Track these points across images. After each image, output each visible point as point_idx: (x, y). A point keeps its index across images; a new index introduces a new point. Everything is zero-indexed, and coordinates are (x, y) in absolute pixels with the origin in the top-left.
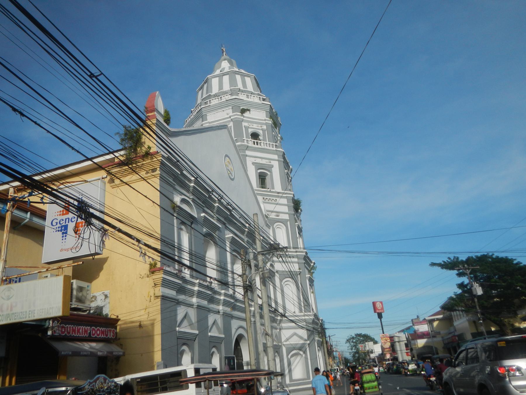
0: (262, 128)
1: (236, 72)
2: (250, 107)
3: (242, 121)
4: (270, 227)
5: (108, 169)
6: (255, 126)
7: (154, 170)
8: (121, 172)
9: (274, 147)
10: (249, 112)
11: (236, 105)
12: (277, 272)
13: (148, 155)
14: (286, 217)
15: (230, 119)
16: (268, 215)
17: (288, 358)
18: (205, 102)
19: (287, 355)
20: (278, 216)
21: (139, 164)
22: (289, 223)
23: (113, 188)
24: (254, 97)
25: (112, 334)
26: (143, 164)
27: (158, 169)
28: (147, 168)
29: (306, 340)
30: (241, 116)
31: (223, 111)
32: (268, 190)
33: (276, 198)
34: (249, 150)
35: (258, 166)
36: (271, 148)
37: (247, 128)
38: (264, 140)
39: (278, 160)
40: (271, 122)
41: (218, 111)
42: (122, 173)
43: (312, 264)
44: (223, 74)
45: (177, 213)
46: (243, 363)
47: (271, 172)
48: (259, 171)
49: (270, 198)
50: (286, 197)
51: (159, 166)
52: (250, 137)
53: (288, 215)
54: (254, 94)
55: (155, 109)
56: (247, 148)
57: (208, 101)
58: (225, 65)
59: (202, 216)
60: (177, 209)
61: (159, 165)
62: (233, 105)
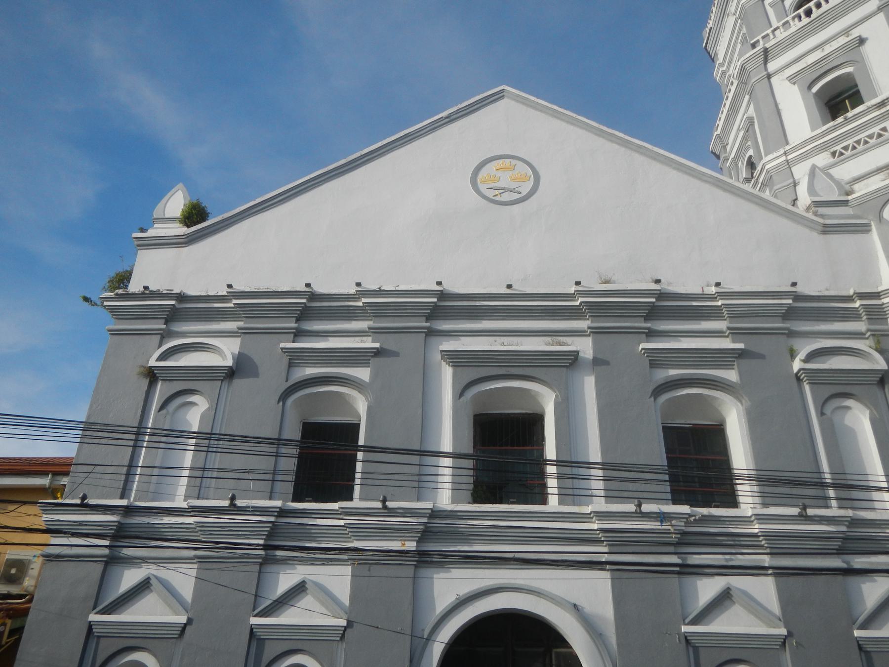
4: (868, 225)
45: (162, 380)
47: (860, 62)
48: (815, 89)
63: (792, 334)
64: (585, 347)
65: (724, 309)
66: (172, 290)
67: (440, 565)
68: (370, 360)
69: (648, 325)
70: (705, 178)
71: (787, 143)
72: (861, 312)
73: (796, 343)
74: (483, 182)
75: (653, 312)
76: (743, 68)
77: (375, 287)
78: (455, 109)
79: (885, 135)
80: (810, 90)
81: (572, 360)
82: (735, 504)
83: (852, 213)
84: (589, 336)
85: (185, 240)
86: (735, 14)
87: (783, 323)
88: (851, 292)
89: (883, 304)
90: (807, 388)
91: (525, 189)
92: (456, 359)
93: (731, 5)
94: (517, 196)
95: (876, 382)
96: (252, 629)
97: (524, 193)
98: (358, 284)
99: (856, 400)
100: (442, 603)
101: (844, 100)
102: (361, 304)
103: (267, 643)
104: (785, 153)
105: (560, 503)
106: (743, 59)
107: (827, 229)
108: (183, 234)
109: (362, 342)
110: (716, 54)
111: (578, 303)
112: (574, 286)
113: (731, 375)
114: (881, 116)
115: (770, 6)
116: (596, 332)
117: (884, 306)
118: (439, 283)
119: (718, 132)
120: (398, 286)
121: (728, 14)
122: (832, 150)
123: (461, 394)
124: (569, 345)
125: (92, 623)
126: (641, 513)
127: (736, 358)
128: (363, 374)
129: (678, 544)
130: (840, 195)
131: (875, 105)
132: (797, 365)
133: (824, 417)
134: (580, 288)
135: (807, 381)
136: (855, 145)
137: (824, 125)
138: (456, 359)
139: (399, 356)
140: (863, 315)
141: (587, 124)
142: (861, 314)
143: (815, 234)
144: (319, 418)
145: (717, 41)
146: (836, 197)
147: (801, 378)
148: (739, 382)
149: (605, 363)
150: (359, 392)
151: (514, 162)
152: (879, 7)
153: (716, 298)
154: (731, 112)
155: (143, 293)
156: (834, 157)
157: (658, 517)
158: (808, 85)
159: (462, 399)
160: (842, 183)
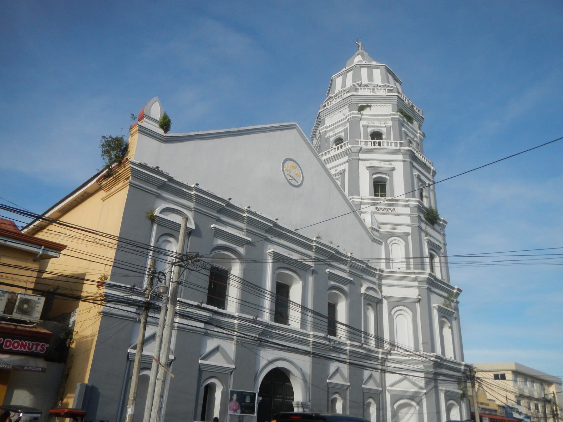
0: (386, 124)
1: (361, 66)
2: (371, 103)
3: (360, 121)
4: (382, 243)
5: (99, 182)
6: (377, 123)
7: (128, 178)
8: (108, 184)
9: (398, 145)
10: (369, 108)
12: (384, 297)
13: (121, 164)
14: (408, 230)
15: (346, 120)
16: (379, 228)
17: (394, 409)
18: (323, 105)
19: (393, 404)
20: (395, 229)
21: (117, 174)
22: (410, 238)
23: (103, 201)
24: (381, 91)
25: (39, 348)
26: (119, 174)
27: (131, 177)
28: (123, 177)
29: (421, 388)
30: (359, 114)
31: (340, 112)
32: (382, 198)
33: (394, 208)
34: (363, 153)
35: (373, 170)
37: (366, 127)
38: (389, 138)
39: (402, 161)
40: (398, 116)
41: (336, 112)
42: (109, 186)
43: (455, 291)
44: (347, 71)
45: (157, 224)
46: (293, 403)
47: (391, 176)
48: (375, 176)
49: (385, 207)
51: (131, 174)
52: (370, 137)
53: (410, 228)
54: (380, 87)
55: (144, 115)
56: (361, 150)
57: (326, 104)
58: (357, 59)
59: (211, 227)
60: (156, 219)
61: (130, 171)
64: (310, 263)
66: (169, 174)
67: (263, 346)
68: (245, 245)
70: (349, 204)
73: (362, 281)
77: (254, 211)
81: (306, 268)
85: (165, 139)
88: (378, 268)
89: (383, 275)
90: (362, 299)
92: (277, 257)
96: (199, 365)
97: (299, 184)
99: (371, 306)
100: (263, 363)
101: (378, 185)
103: (203, 373)
104: (361, 199)
105: (301, 328)
107: (374, 240)
108: (165, 136)
110: (324, 119)
116: (317, 260)
125: (129, 354)
128: (241, 250)
129: (330, 350)
132: (363, 290)
134: (317, 240)
138: (277, 257)
143: (370, 240)
146: (376, 228)
149: (317, 273)
151: (296, 165)
155: (154, 169)
160: (378, 222)
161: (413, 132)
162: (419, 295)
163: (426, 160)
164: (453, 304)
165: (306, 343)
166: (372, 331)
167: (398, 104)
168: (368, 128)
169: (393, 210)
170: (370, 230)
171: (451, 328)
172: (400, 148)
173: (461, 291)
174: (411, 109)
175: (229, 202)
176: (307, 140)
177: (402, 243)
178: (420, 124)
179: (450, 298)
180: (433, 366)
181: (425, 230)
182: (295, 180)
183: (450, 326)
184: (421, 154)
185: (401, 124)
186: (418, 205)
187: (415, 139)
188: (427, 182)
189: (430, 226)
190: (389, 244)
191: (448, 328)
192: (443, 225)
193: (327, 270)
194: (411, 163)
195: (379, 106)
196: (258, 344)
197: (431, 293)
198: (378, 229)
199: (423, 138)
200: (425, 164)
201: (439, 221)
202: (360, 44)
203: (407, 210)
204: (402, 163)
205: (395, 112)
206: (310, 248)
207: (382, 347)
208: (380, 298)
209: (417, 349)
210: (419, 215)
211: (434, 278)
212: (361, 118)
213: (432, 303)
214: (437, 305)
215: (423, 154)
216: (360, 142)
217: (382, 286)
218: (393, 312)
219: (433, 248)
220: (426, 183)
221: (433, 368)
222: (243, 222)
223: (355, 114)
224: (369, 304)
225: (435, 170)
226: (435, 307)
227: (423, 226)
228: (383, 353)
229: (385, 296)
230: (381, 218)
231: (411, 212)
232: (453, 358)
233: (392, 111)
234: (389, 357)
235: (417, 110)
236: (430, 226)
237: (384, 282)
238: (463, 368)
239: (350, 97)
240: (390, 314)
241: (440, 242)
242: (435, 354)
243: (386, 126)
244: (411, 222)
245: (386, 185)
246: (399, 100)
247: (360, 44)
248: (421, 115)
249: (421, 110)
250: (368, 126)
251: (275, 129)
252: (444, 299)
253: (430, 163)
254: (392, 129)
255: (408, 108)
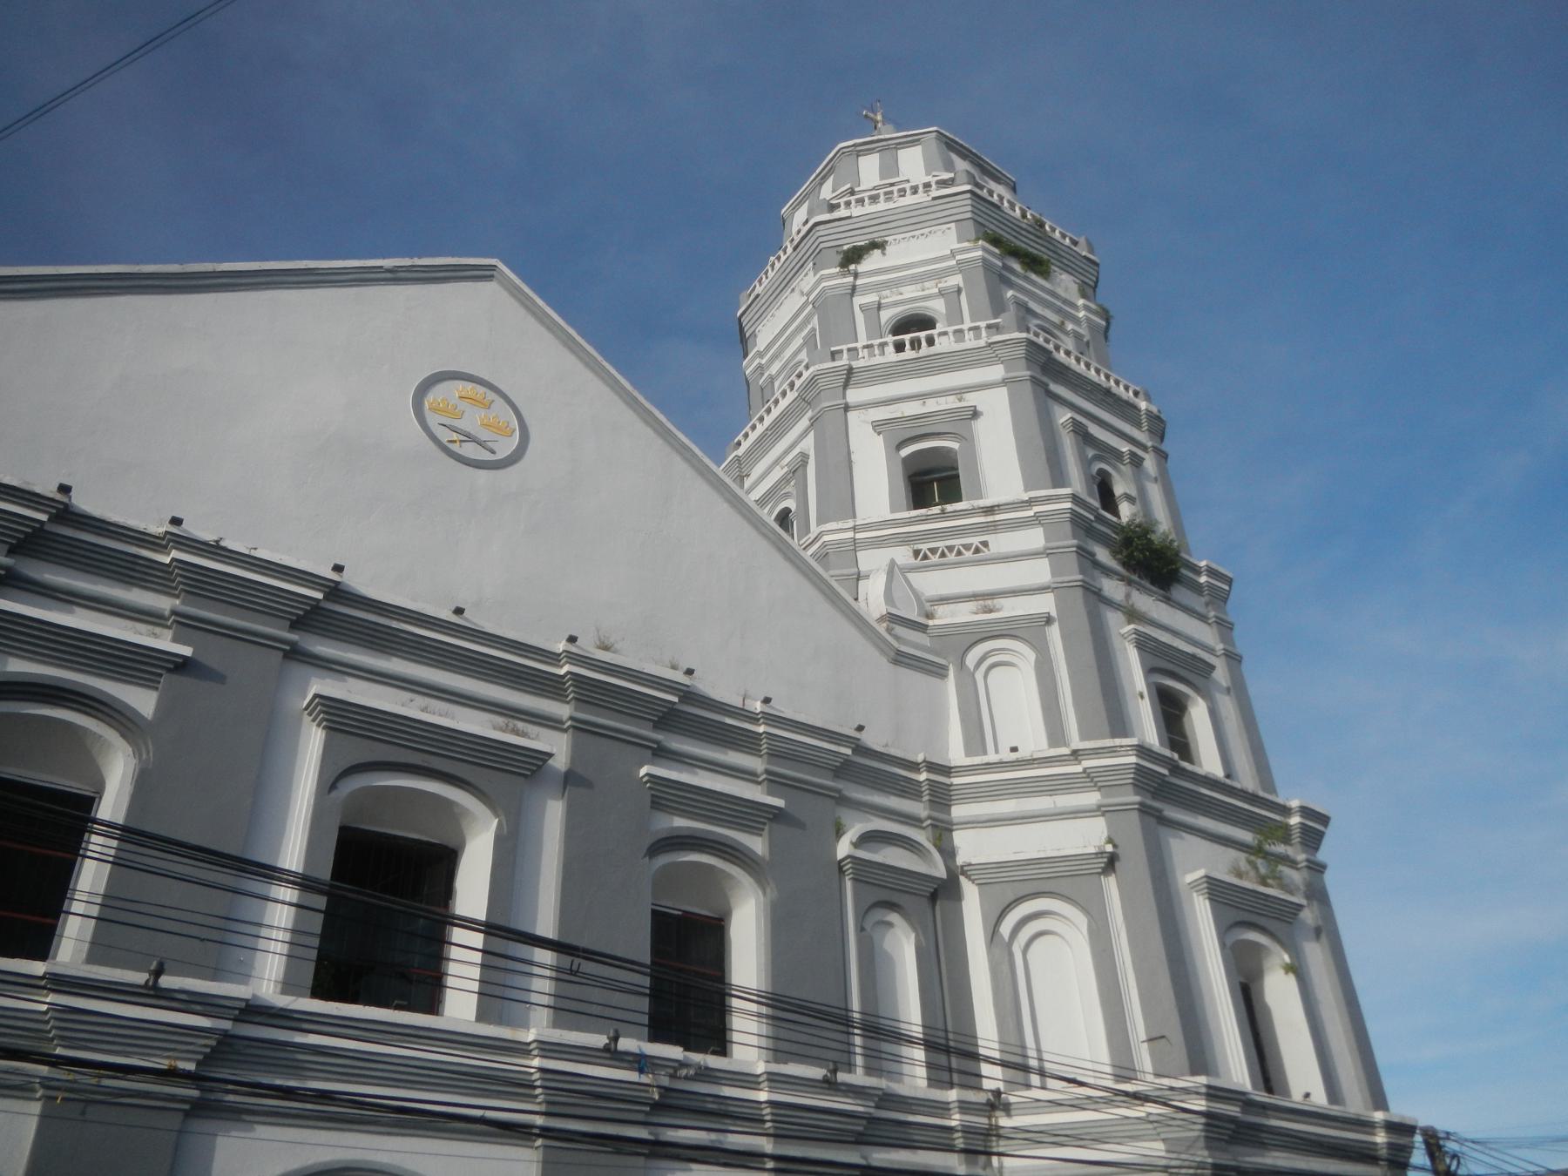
4: (945, 668)
6: (910, 292)
10: (880, 251)
11: (822, 246)
14: (1045, 604)
15: (811, 306)
16: (930, 616)
20: (991, 611)
22: (1054, 632)
30: (844, 276)
31: (793, 290)
32: (930, 513)
36: (970, 342)
40: (979, 253)
43: (1295, 820)
47: (967, 439)
49: (949, 543)
50: (1037, 520)
62: (812, 256)
63: (843, 800)
64: (558, 747)
65: (764, 741)
67: (237, 1115)
68: (161, 675)
69: (659, 736)
71: (854, 516)
72: (923, 789)
73: (846, 815)
74: (434, 410)
75: (668, 719)
76: (813, 380)
77: (209, 537)
78: (406, 262)
79: (984, 552)
80: (899, 451)
81: (532, 764)
82: (722, 1048)
83: (929, 645)
84: (565, 731)
86: (808, 295)
87: (833, 781)
88: (920, 758)
89: (951, 785)
90: (849, 885)
91: (505, 448)
92: (337, 716)
93: (802, 279)
94: (486, 456)
95: (928, 894)
97: (500, 456)
98: (176, 521)
99: (902, 915)
101: (931, 482)
102: (167, 560)
104: (854, 528)
105: (482, 1016)
106: (817, 367)
107: (901, 659)
109: (155, 635)
110: (754, 335)
111: (562, 672)
112: (564, 642)
113: (757, 844)
114: (986, 525)
115: (861, 309)
116: (580, 728)
117: (952, 788)
118: (338, 569)
119: (741, 451)
120: (255, 549)
121: (793, 290)
122: (916, 547)
123: (333, 787)
124: (533, 739)
126: (616, 1052)
127: (769, 819)
128: (142, 701)
129: (657, 1107)
130: (919, 615)
131: (983, 508)
132: (844, 848)
133: (863, 933)
134: (573, 649)
135: (851, 876)
136: (946, 551)
137: (909, 509)
138: (337, 716)
139: (223, 683)
140: (925, 793)
141: (617, 381)
142: (922, 792)
143: (884, 661)
144: (44, 777)
145: (762, 318)
146: (914, 615)
147: (845, 868)
148: (767, 857)
150: (123, 736)
151: (491, 395)
152: (1004, 379)
153: (758, 720)
154: (770, 433)
156: (916, 559)
157: (633, 1062)
158: (897, 443)
159: (334, 794)
160: (923, 598)
161: (1059, 303)
162: (1110, 841)
163: (1117, 383)
164: (1296, 877)
165: (518, 1085)
166: (910, 1013)
167: (976, 217)
168: (882, 313)
169: (980, 546)
170: (881, 628)
171: (1297, 969)
172: (990, 341)
173: (1324, 820)
174: (1039, 234)
175: (66, 505)
176: (548, 316)
177: (1025, 656)
178: (1082, 281)
179: (1267, 847)
180: (1206, 1137)
181: (1124, 604)
182: (481, 444)
183: (1287, 964)
184: (1099, 367)
185: (998, 279)
186: (1073, 512)
187: (1070, 326)
188: (1124, 450)
189: (1149, 593)
190: (972, 668)
191: (1282, 972)
192: (1210, 586)
193: (643, 771)
194: (1034, 380)
195: (913, 237)
196: (187, 1107)
197: (1164, 832)
198: (922, 620)
199: (1104, 323)
200: (1108, 392)
201: (1184, 571)
202: (879, 117)
203: (1035, 538)
204: (1004, 391)
205: (968, 241)
206: (550, 686)
207: (972, 1080)
208: (940, 871)
209: (1124, 1072)
210: (1079, 547)
211: (1170, 770)
212: (854, 288)
213: (1178, 873)
214: (1201, 873)
215: (1109, 368)
216: (845, 352)
217: (951, 831)
218: (1006, 928)
219: (1170, 667)
220: (1123, 453)
221: (1208, 1148)
222: (165, 589)
223: (831, 277)
224: (892, 906)
225: (1154, 409)
226: (1193, 885)
227: (1113, 589)
228: (965, 1107)
229: (962, 867)
230: (932, 583)
231: (1047, 540)
232: (1320, 1099)
233: (958, 243)
234: (1004, 1122)
235: (1067, 240)
236: (1150, 590)
237: (959, 811)
238: (1381, 1138)
239: (811, 234)
240: (993, 934)
241: (1211, 651)
242: (1202, 1080)
243: (941, 294)
244: (1053, 575)
245: (957, 477)
246: (975, 204)
247: (879, 117)
248: (1084, 253)
249: (1082, 240)
250: (879, 307)
251: (389, 275)
252: (1247, 855)
253: (1136, 394)
254: (963, 297)
255: (1024, 233)
